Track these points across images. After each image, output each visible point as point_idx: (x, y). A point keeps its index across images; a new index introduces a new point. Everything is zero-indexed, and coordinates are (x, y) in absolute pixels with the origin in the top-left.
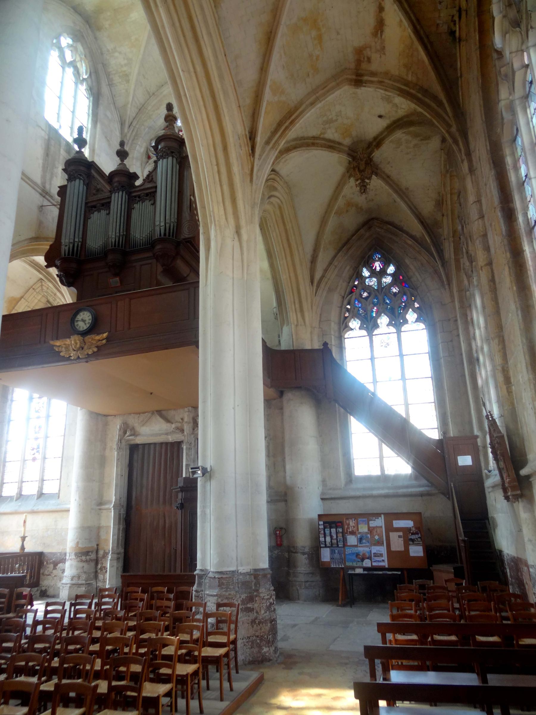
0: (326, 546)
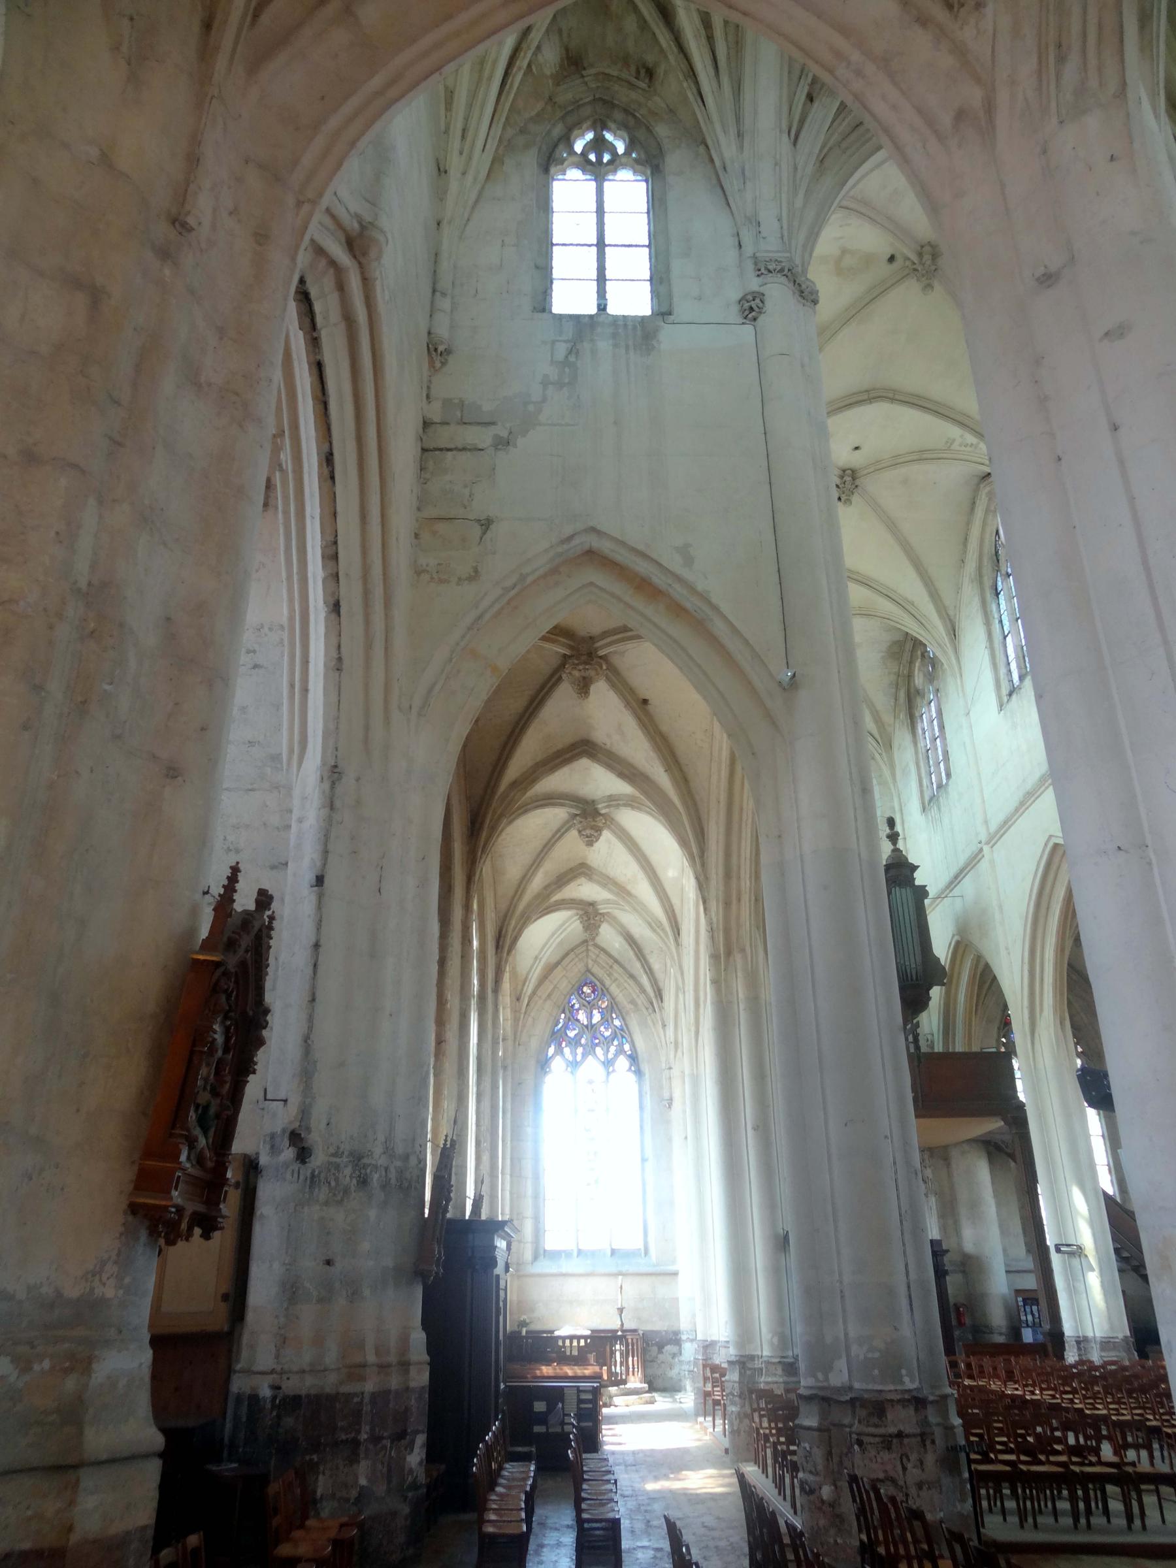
0: (1028, 1326)
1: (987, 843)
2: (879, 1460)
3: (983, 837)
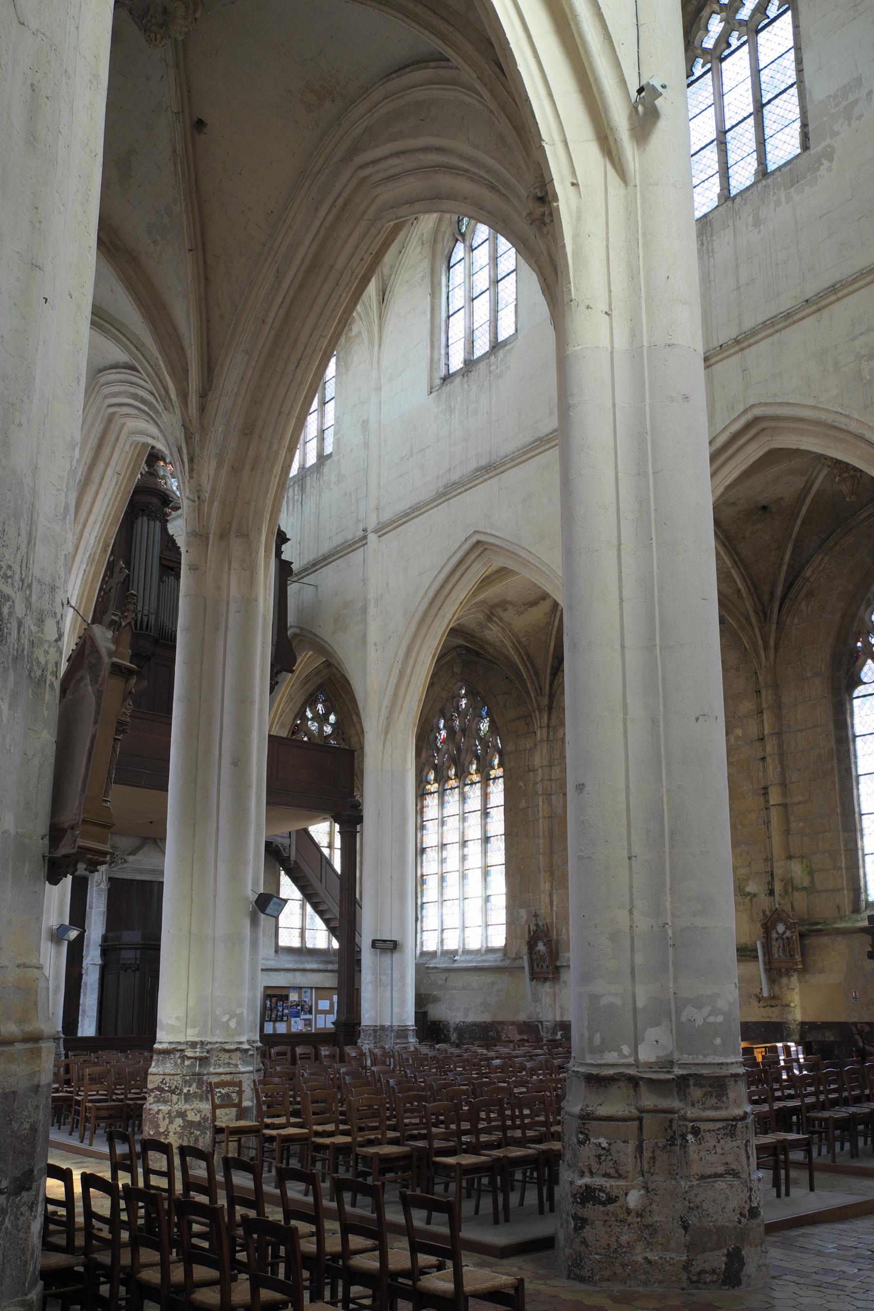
1: (376, 531)
2: (719, 1151)
3: (372, 523)
